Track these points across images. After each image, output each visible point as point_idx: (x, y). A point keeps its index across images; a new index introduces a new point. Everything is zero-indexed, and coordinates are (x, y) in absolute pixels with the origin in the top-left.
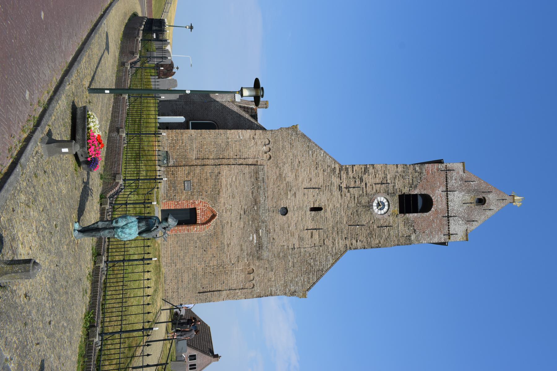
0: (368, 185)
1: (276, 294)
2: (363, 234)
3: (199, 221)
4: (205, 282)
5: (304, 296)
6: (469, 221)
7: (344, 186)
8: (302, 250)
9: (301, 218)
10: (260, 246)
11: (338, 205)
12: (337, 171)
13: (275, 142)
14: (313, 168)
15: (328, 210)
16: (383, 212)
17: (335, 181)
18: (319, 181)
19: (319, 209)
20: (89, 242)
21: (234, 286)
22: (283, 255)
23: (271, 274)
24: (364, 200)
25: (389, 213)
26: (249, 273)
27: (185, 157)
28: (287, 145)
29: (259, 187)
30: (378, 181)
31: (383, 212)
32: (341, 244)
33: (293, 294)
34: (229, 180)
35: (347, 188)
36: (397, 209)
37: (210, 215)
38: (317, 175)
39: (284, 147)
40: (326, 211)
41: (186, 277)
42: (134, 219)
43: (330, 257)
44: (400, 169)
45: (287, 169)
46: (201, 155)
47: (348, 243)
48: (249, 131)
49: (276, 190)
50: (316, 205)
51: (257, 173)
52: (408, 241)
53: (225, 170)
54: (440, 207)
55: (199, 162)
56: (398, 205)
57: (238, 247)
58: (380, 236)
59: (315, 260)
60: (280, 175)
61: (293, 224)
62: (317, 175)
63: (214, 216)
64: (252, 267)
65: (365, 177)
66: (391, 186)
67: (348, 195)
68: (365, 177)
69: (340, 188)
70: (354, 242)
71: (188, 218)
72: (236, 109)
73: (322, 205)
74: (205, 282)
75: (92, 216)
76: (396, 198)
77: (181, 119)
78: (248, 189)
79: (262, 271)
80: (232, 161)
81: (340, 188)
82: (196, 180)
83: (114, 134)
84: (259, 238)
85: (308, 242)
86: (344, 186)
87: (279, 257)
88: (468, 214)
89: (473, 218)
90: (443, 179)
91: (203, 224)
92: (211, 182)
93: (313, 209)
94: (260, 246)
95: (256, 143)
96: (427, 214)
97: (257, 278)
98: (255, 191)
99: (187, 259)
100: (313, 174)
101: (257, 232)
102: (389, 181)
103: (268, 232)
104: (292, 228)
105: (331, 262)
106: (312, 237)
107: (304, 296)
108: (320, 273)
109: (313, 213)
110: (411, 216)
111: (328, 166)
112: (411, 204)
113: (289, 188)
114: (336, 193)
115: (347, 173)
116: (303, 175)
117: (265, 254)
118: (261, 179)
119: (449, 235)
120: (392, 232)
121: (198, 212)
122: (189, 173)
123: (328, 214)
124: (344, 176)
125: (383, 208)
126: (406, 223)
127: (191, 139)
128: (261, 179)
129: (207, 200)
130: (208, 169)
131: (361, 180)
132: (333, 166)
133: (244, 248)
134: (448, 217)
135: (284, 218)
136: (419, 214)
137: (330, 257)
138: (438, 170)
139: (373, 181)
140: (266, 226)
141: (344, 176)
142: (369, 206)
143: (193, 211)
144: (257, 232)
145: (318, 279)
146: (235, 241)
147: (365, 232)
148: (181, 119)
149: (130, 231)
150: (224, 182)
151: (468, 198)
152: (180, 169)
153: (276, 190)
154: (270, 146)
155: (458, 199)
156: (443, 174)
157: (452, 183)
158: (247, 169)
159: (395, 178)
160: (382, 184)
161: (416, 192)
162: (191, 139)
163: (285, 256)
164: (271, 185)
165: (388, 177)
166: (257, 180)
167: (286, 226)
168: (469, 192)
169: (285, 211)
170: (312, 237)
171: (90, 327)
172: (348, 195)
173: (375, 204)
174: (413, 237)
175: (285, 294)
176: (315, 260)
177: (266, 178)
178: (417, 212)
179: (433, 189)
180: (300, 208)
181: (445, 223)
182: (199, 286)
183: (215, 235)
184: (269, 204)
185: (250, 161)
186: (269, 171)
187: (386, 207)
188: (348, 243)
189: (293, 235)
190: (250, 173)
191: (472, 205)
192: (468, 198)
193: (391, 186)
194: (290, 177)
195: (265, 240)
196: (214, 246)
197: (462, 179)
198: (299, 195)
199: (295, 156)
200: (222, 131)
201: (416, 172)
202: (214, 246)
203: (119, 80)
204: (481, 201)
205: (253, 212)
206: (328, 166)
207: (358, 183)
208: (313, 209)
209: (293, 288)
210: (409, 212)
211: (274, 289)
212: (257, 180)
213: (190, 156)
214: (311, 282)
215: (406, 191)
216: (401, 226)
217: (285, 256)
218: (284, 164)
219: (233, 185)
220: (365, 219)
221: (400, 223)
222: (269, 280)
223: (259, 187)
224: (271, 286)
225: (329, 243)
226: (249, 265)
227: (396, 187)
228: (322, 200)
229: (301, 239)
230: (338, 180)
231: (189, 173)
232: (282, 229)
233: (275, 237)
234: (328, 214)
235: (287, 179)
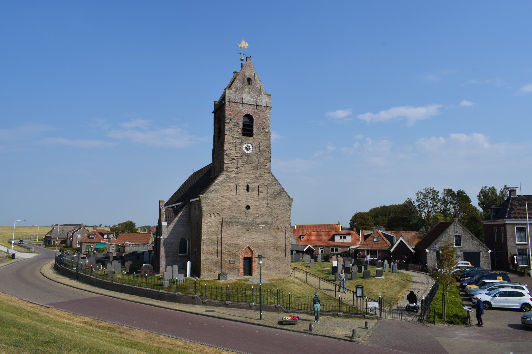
0: (236, 155)
1: (290, 215)
2: (263, 161)
3: (251, 256)
4: (280, 253)
5: (292, 199)
6: (260, 92)
7: (236, 170)
8: (269, 199)
9: (252, 199)
10: (266, 223)
11: (247, 175)
12: (228, 173)
13: (210, 211)
14: (225, 188)
15: (248, 181)
16: (251, 147)
17: (233, 175)
18: (232, 184)
19: (248, 186)
20: (321, 318)
21: (284, 237)
22: (271, 210)
23: (280, 217)
24: (245, 158)
25: (252, 144)
26: (278, 229)
27: (216, 263)
28: (212, 203)
29: (235, 222)
30: (234, 149)
31: (251, 147)
32: (267, 176)
33: (290, 206)
34: (230, 238)
35: (237, 168)
36: (251, 138)
37: (248, 250)
38: (229, 186)
39: (213, 206)
40: (249, 183)
41: (277, 263)
42: (315, 305)
43: (273, 183)
45: (225, 205)
46: (215, 254)
47: (267, 171)
48: (202, 226)
49: (236, 212)
50: (246, 188)
51: (227, 223)
52: (268, 134)
53: (225, 241)
54: (251, 110)
55: (219, 255)
56: (248, 137)
57: (266, 235)
58: (265, 151)
59: (275, 192)
60: (228, 208)
61: (255, 203)
62: (229, 186)
63: (249, 248)
64: (275, 228)
65: (232, 156)
66: (237, 140)
67: (241, 168)
68: (232, 156)
69: (237, 173)
70: (267, 167)
71: (248, 263)
72: (172, 226)
73: (246, 185)
74: (280, 253)
75: (313, 318)
76: (245, 138)
78: (235, 228)
79: (278, 222)
80: (220, 236)
81: (237, 173)
82: (230, 257)
83: (253, 308)
84: (261, 223)
85: (265, 195)
86: (236, 170)
87: (271, 212)
88: (256, 91)
89: (258, 89)
90: (235, 105)
91: (252, 253)
92: (231, 249)
93: (248, 190)
94: (266, 223)
95: (210, 222)
96: (254, 119)
97: (281, 225)
98: (237, 224)
99: (269, 263)
100: (228, 188)
101: (258, 224)
102: (235, 141)
103: (258, 218)
104: (257, 203)
105: (276, 182)
106: (262, 192)
107: (292, 199)
108: (282, 189)
109: (250, 190)
110: (255, 129)
111: (224, 179)
113: (235, 204)
114: (240, 175)
115: (229, 167)
116: (228, 194)
117: (270, 220)
118: (230, 220)
119: (267, 107)
120: (263, 143)
121: (246, 256)
122: (225, 261)
123: (251, 181)
124: (230, 170)
126: (258, 133)
127: (206, 260)
128: (230, 220)
129: (240, 251)
130: (224, 250)
131: (233, 159)
132: (224, 176)
133: (266, 231)
134: (257, 105)
135: (251, 208)
136: (254, 124)
137: (273, 183)
138: (229, 107)
139: (234, 151)
140: (256, 219)
141: (230, 170)
142: (248, 155)
143: (245, 259)
144: (258, 224)
145: (285, 191)
146: (262, 237)
147: (262, 160)
149: (318, 306)
150: (231, 242)
151: (247, 90)
152: (223, 266)
153: (236, 212)
154: (212, 213)
155: (247, 97)
156: (232, 104)
157: (237, 99)
158: (225, 228)
159: (233, 137)
160: (236, 146)
161: (242, 124)
162: (206, 260)
163: (271, 209)
164: (234, 214)
165: (232, 141)
166: (232, 222)
167: (256, 207)
168: (243, 89)
169: (248, 207)
170: (262, 192)
171: (338, 316)
172: (241, 168)
173: (247, 152)
174: (267, 130)
175: (290, 210)
176: (275, 192)
177: (230, 217)
178: (253, 126)
179: (241, 113)
180: (247, 198)
181: (260, 108)
182: (282, 256)
183: (258, 248)
184: (244, 216)
185: (220, 226)
186: (226, 214)
187: (249, 145)
188: (267, 171)
189: (260, 204)
190: (227, 227)
191: (251, 87)
193: (237, 140)
194: (230, 203)
195: (263, 220)
196: (264, 248)
197: (235, 92)
198: (240, 198)
199: (218, 199)
200: (202, 242)
201: (229, 122)
202: (264, 248)
203: (256, 310)
204: (249, 80)
205: (248, 226)
206: (224, 179)
207: (234, 161)
208: (248, 190)
209: (288, 206)
210: (252, 131)
211: (287, 216)
212: (232, 222)
213: (216, 260)
214: (285, 195)
215: (240, 131)
216: (260, 137)
217: (271, 209)
218: (222, 206)
219: (231, 236)
220: (255, 159)
221: (258, 137)
222: (282, 218)
223: (235, 222)
224: (286, 217)
225: (266, 183)
226: (274, 229)
227: (238, 137)
228: (243, 185)
229: (263, 199)
230: (232, 174)
231: (225, 261)
232: (257, 209)
233: (261, 214)
234: (251, 181)
235: (231, 204)
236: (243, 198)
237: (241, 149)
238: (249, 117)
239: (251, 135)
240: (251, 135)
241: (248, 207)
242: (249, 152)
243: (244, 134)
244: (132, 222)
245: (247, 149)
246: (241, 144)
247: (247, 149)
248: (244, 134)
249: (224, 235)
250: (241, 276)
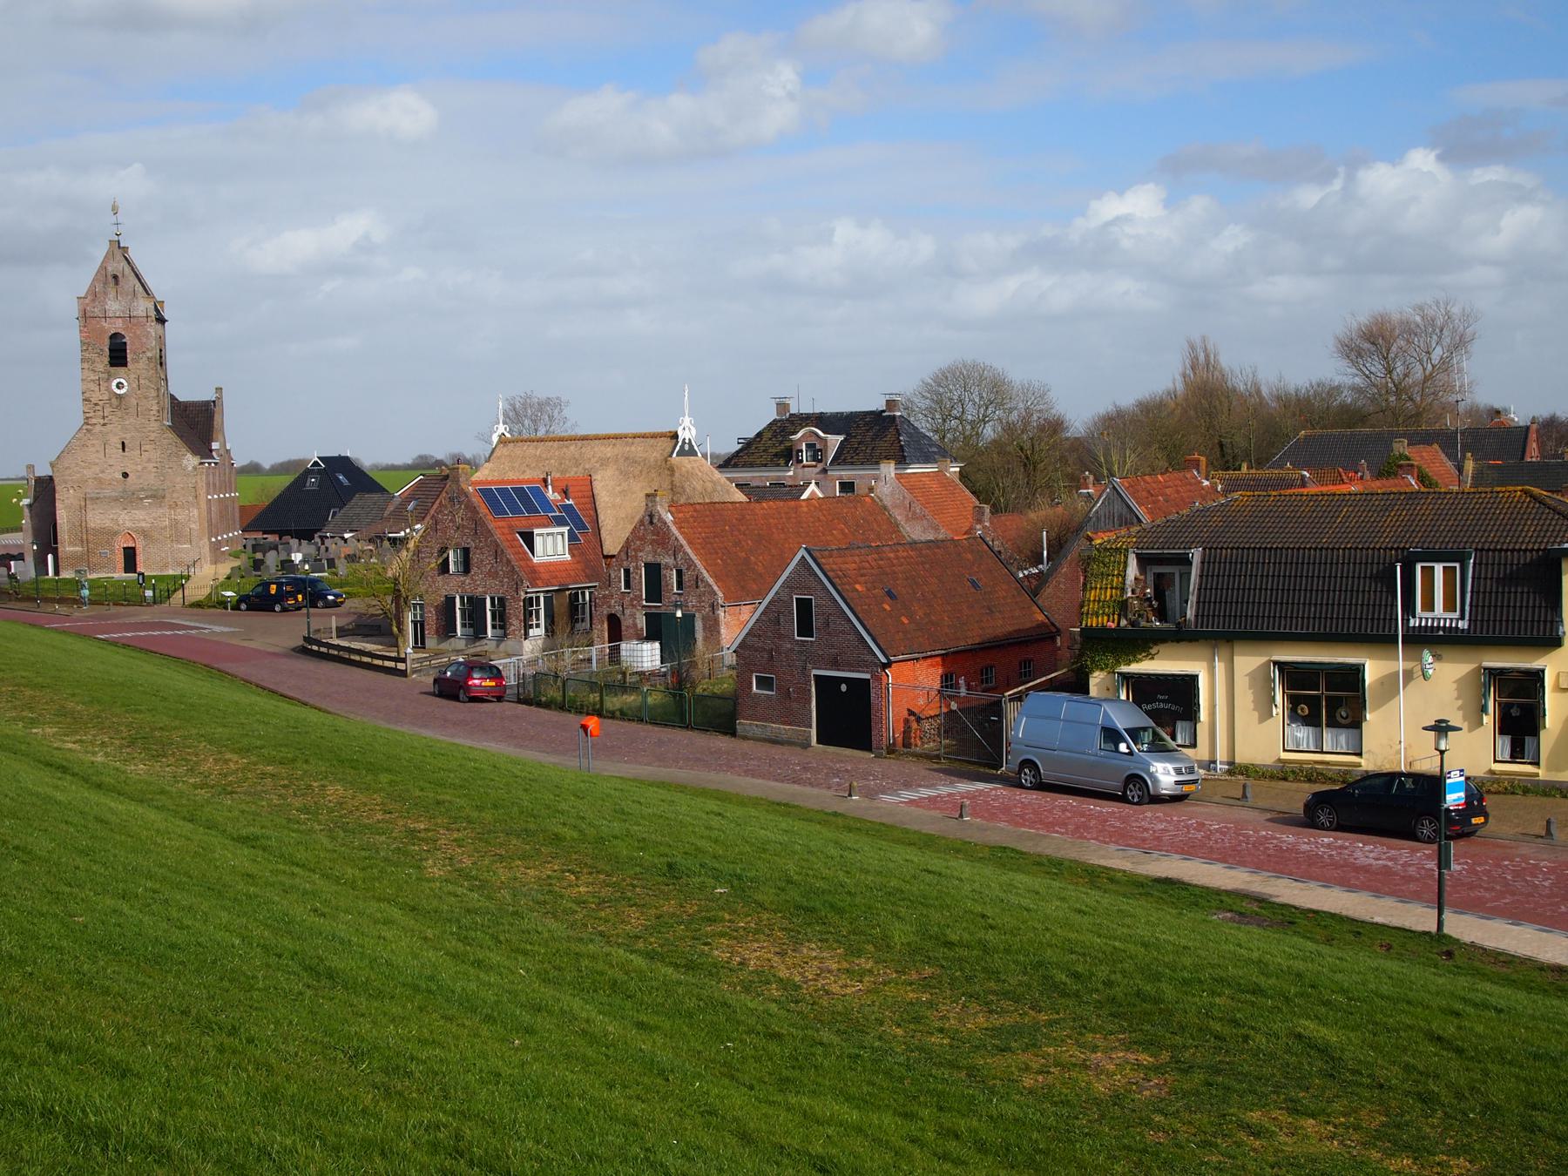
17: (98, 428)
23: (178, 487)
36: (122, 370)
44: (86, 365)
65: (94, 400)
68: (94, 400)
71: (130, 557)
76: (113, 370)
77: (50, 557)
112: (118, 355)
123: (128, 436)
125: (121, 382)
126: (136, 361)
130: (91, 538)
142: (119, 397)
148: (50, 557)
151: (112, 295)
169: (125, 475)
174: (149, 354)
179: (103, 330)
192: (112, 295)
194: (97, 469)
204: (115, 277)
215: (107, 360)
221: (138, 364)
225: (153, 436)
229: (149, 460)
234: (128, 436)
236: (119, 460)
237: (109, 389)
238: (115, 337)
239: (125, 364)
240: (125, 364)
241: (125, 475)
242: (122, 391)
243: (112, 364)
244: (340, 464)
245: (119, 386)
246: (108, 380)
247: (119, 386)
248: (112, 364)
249: (90, 515)
250: (119, 575)
